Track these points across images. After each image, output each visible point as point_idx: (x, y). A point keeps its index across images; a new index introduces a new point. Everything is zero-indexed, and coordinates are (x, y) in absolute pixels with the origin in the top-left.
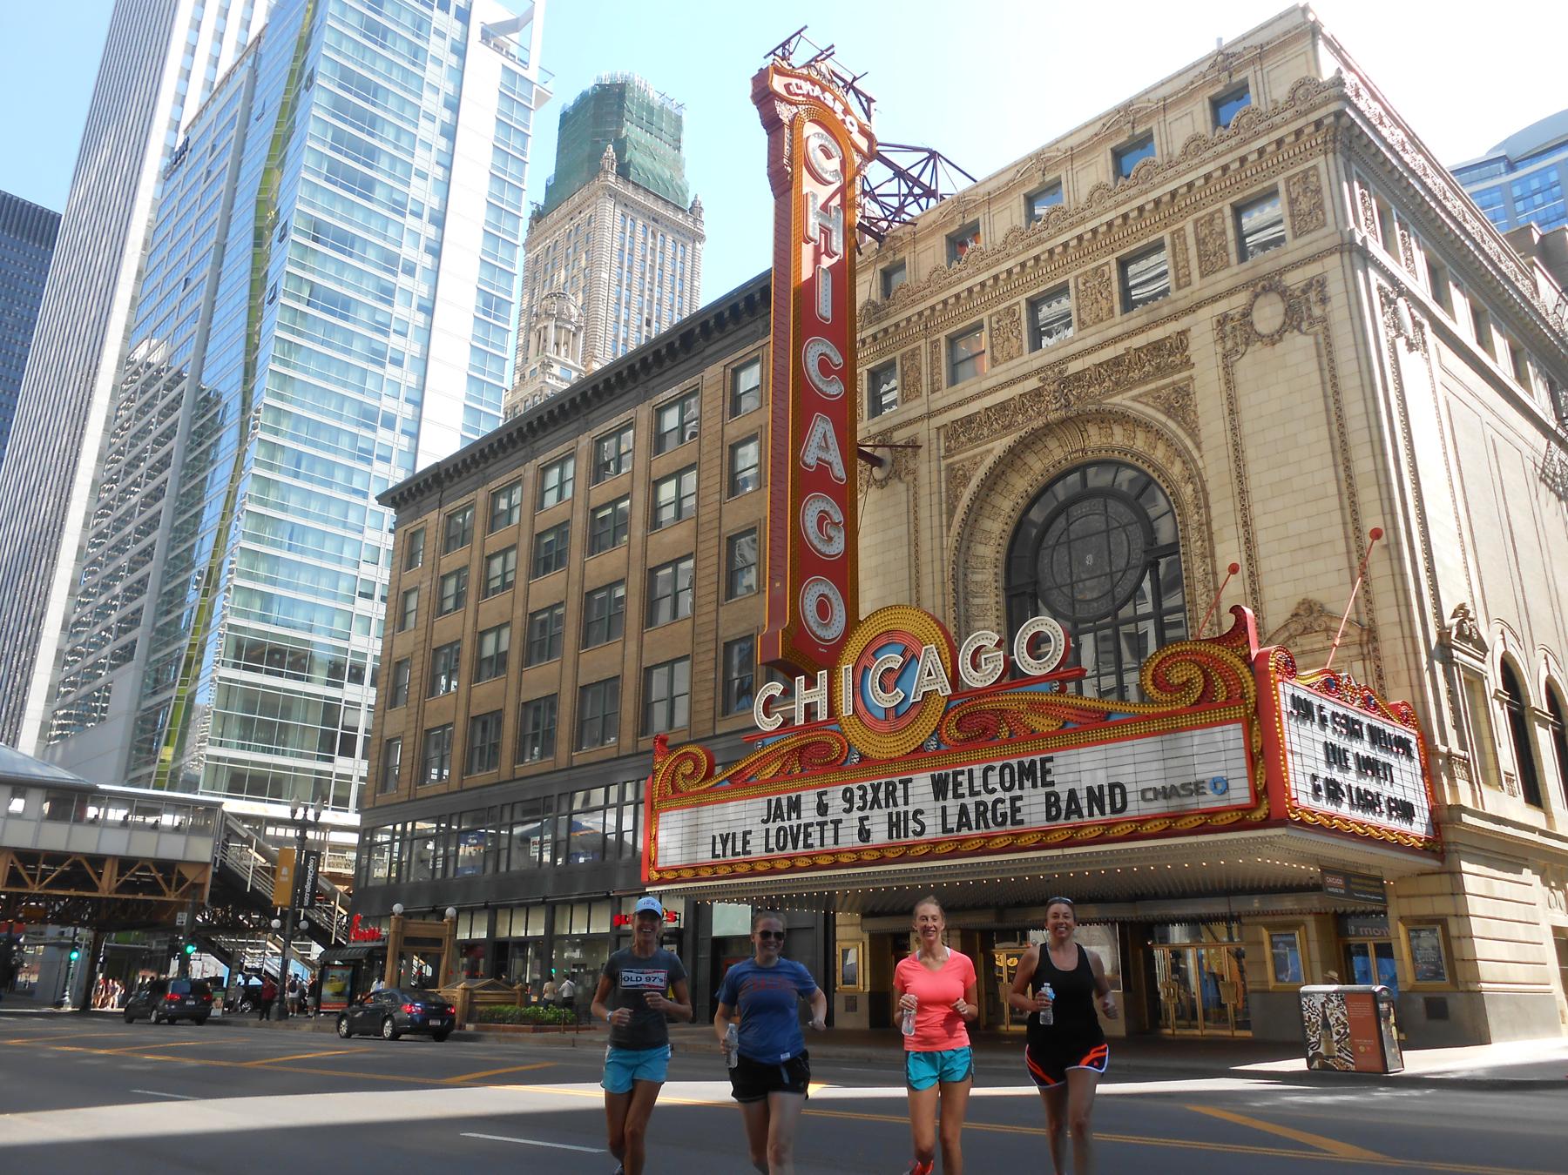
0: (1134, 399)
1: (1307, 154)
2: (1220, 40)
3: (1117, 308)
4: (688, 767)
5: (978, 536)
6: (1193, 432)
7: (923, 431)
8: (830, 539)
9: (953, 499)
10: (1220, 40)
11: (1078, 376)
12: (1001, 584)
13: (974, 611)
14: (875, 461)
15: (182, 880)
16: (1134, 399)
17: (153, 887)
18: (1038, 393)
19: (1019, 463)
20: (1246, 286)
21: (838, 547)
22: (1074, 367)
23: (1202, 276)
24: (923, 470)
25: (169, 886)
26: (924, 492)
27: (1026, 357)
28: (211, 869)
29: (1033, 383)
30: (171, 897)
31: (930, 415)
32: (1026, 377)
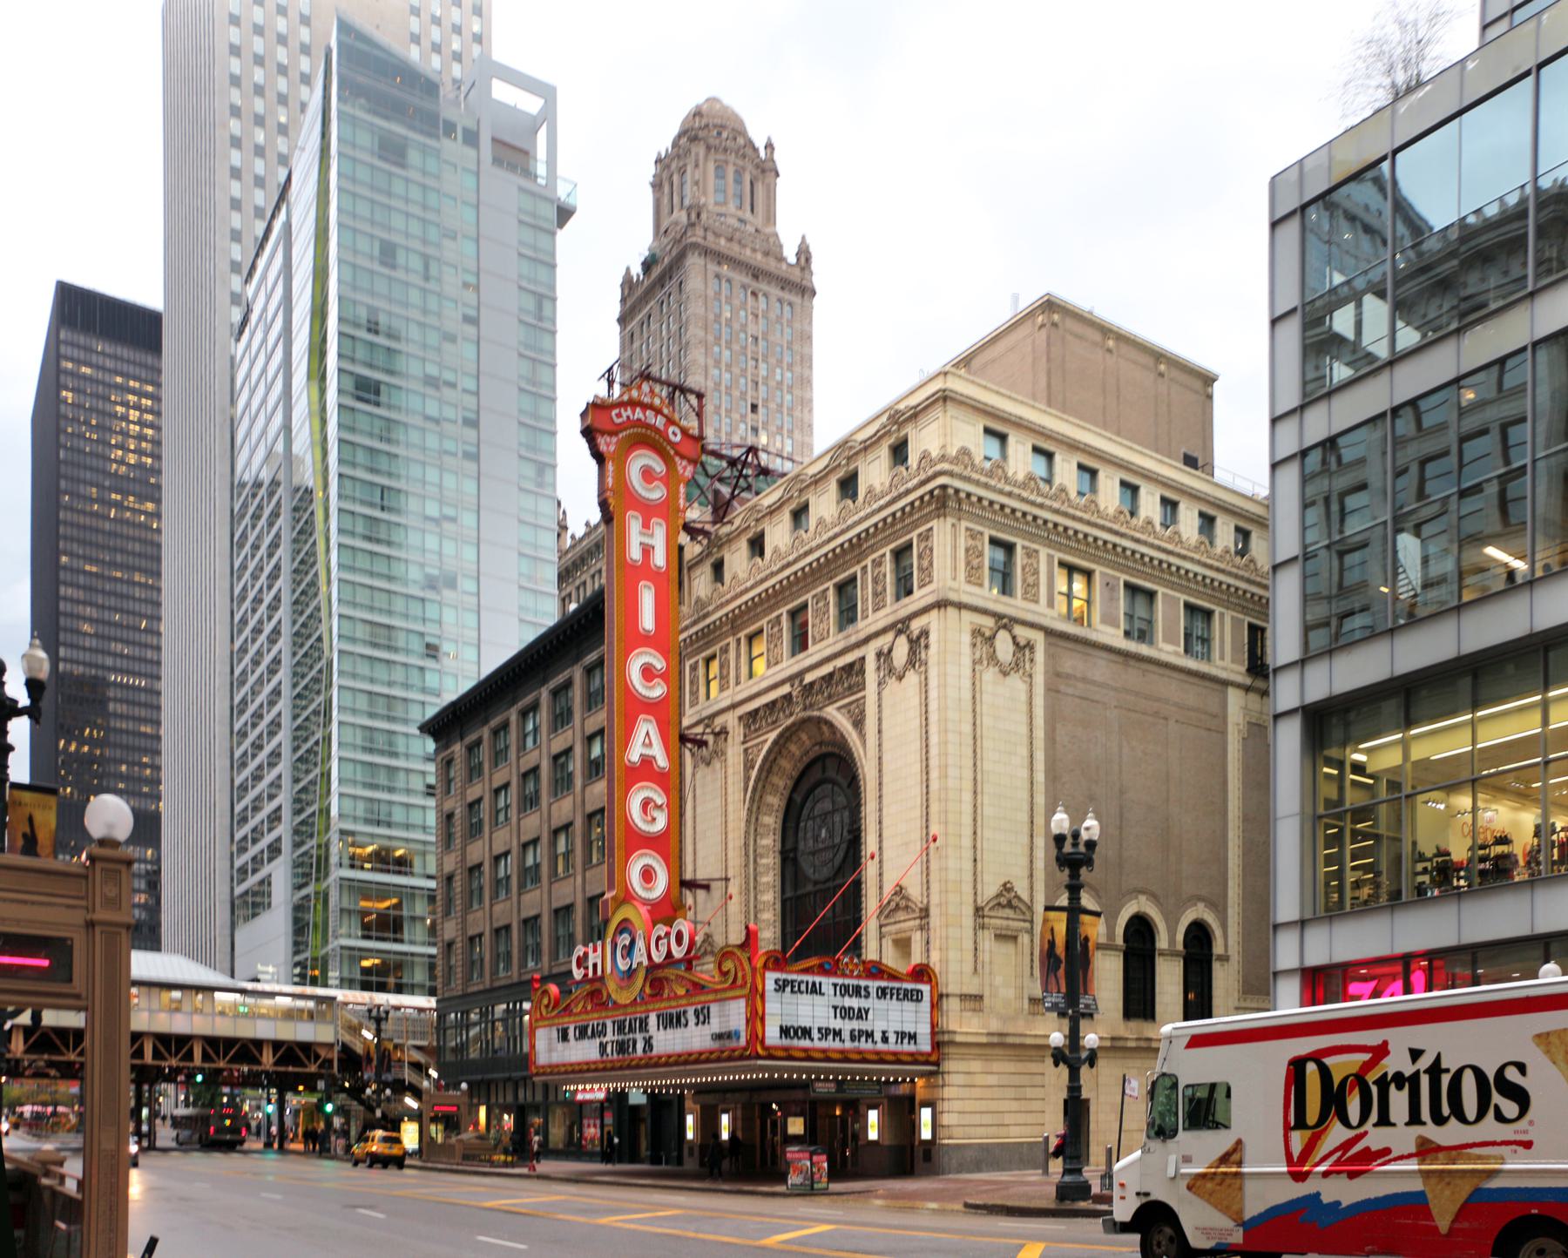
0: (839, 709)
1: (927, 518)
2: (1016, 298)
3: (890, 590)
4: (545, 1001)
5: (764, 809)
6: (864, 743)
7: (731, 720)
8: (654, 819)
9: (747, 779)
10: (1016, 298)
11: (812, 684)
12: (778, 846)
13: (760, 869)
14: (702, 744)
15: (317, 1057)
16: (839, 709)
17: (297, 1062)
18: (788, 698)
19: (784, 752)
20: (892, 626)
21: (661, 823)
22: (809, 678)
23: (875, 611)
24: (730, 752)
25: (309, 1058)
26: (730, 771)
27: (784, 664)
28: (337, 1049)
29: (786, 689)
30: (313, 1068)
31: (734, 706)
32: (782, 682)
